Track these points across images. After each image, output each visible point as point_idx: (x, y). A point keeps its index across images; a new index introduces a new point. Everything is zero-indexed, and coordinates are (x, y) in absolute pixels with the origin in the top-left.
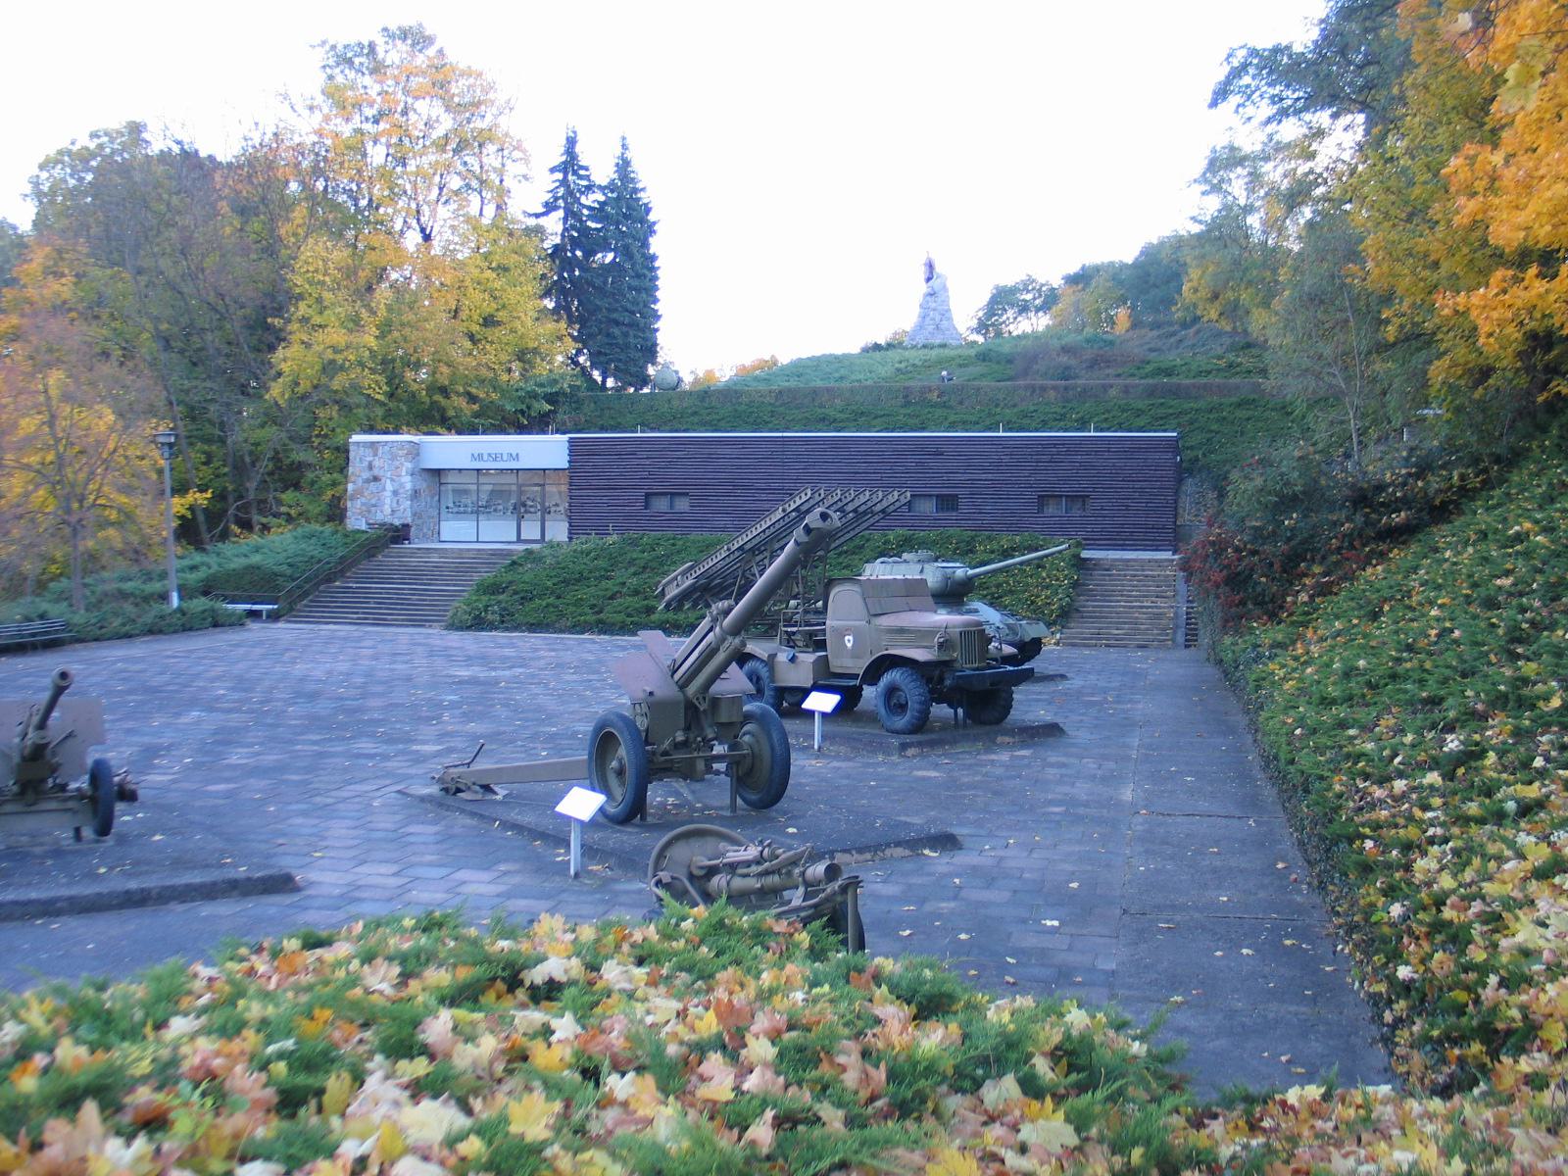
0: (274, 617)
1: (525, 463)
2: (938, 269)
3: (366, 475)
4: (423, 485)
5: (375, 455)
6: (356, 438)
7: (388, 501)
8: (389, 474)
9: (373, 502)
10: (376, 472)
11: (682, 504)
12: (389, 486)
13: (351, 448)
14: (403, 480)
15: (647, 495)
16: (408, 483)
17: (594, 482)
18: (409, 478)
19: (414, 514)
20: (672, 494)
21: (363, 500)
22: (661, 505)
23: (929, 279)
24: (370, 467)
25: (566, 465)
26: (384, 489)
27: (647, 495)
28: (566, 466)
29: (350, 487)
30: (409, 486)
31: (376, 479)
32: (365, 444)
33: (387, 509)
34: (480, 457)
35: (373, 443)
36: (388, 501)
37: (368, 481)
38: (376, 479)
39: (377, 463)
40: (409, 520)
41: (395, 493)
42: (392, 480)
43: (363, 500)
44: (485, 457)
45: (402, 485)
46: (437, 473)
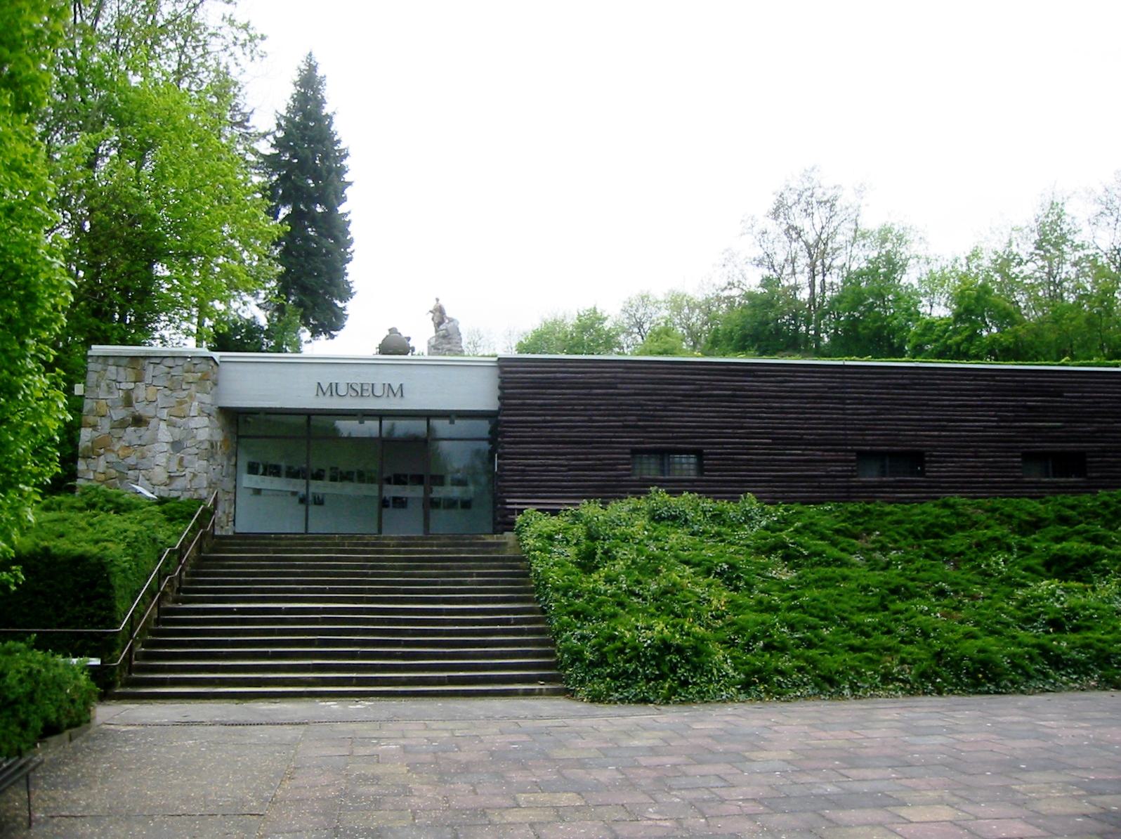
2: (449, 314)
3: (119, 413)
6: (97, 349)
8: (164, 414)
9: (132, 460)
10: (140, 409)
12: (165, 434)
13: (92, 366)
14: (193, 424)
17: (547, 432)
21: (112, 457)
23: (438, 325)
24: (128, 401)
26: (154, 440)
30: (203, 435)
31: (139, 421)
34: (333, 389)
36: (161, 459)
37: (122, 424)
38: (139, 421)
39: (141, 392)
41: (176, 445)
42: (171, 424)
43: (112, 457)
44: (342, 391)
45: (191, 433)
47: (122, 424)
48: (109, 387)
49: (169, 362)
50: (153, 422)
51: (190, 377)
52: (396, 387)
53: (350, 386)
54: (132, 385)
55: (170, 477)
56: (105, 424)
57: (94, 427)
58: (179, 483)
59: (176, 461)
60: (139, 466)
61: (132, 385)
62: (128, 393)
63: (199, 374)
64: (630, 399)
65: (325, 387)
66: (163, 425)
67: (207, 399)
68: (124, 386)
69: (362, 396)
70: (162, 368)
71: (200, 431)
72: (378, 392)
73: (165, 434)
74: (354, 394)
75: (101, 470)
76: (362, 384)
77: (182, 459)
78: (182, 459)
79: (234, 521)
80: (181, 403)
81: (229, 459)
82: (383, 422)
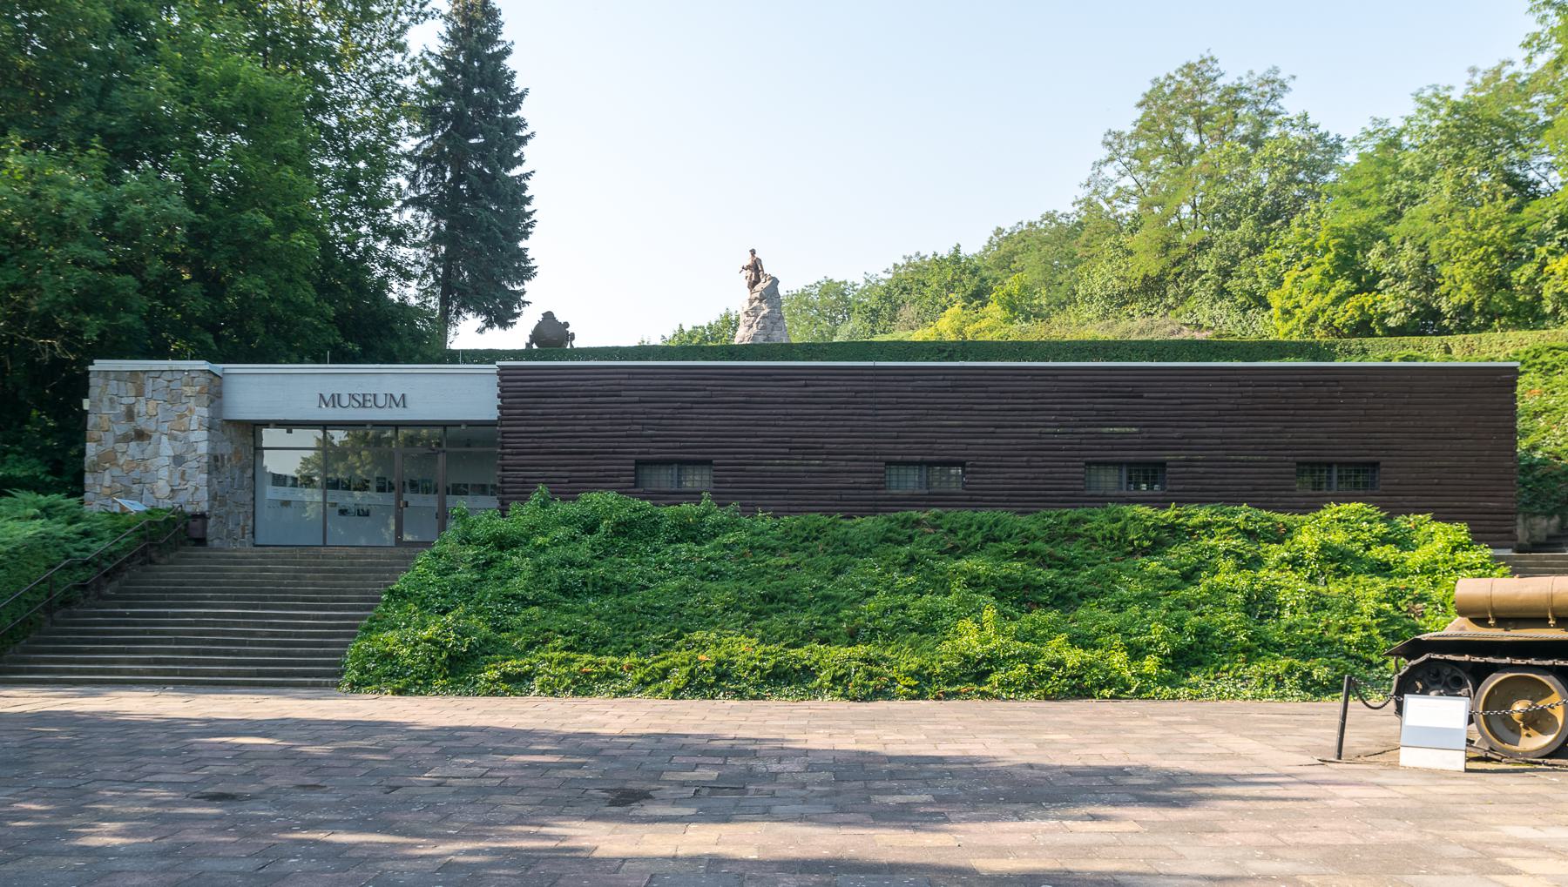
1: (415, 412)
3: (123, 428)
4: (226, 449)
5: (140, 393)
9: (135, 475)
10: (141, 423)
12: (167, 449)
13: (93, 381)
14: (193, 437)
16: (200, 441)
18: (204, 434)
19: (213, 497)
24: (130, 415)
25: (493, 414)
26: (157, 454)
29: (91, 449)
30: (203, 448)
31: (141, 435)
32: (119, 376)
33: (163, 488)
34: (335, 400)
36: (164, 473)
37: (126, 439)
38: (141, 435)
39: (141, 407)
40: (204, 507)
41: (178, 460)
42: (173, 438)
43: (117, 472)
44: (345, 402)
45: (191, 446)
46: (252, 429)
47: (126, 439)
48: (111, 400)
49: (168, 376)
50: (155, 436)
51: (188, 390)
52: (398, 397)
53: (352, 396)
54: (133, 400)
55: (172, 490)
56: (109, 440)
57: (98, 441)
59: (178, 474)
60: (143, 480)
61: (133, 400)
63: (198, 388)
64: (639, 408)
65: (327, 398)
66: (165, 439)
68: (126, 401)
69: (364, 406)
70: (162, 382)
71: (200, 445)
72: (381, 402)
73: (167, 449)
74: (356, 405)
75: (107, 483)
76: (364, 395)
77: (184, 473)
78: (184, 473)
79: (253, 533)
80: (181, 417)
82: (264, 446)
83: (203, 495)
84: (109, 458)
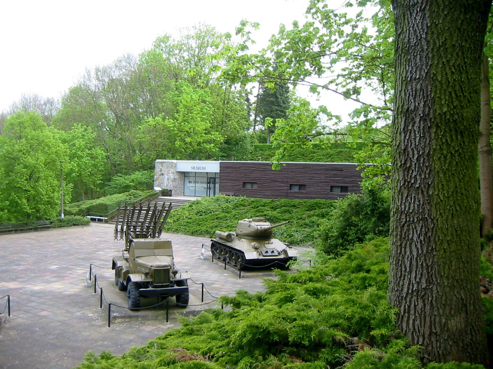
0: (106, 222)
3: (160, 173)
6: (158, 160)
7: (166, 182)
8: (166, 173)
9: (161, 182)
10: (162, 172)
11: (255, 186)
12: (166, 177)
15: (244, 183)
17: (228, 178)
20: (252, 183)
22: (248, 186)
24: (161, 171)
27: (244, 183)
28: (219, 172)
30: (172, 177)
31: (163, 174)
34: (194, 167)
35: (162, 163)
36: (166, 182)
37: (160, 175)
38: (163, 174)
39: (163, 169)
41: (168, 179)
42: (167, 175)
45: (170, 176)
51: (170, 166)
56: (158, 175)
58: (168, 186)
62: (161, 169)
67: (173, 170)
81: (181, 181)
83: (172, 186)
84: (157, 178)
